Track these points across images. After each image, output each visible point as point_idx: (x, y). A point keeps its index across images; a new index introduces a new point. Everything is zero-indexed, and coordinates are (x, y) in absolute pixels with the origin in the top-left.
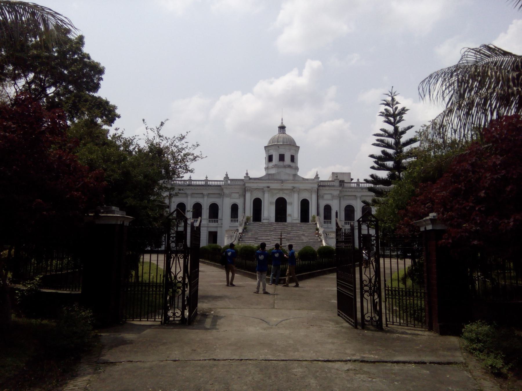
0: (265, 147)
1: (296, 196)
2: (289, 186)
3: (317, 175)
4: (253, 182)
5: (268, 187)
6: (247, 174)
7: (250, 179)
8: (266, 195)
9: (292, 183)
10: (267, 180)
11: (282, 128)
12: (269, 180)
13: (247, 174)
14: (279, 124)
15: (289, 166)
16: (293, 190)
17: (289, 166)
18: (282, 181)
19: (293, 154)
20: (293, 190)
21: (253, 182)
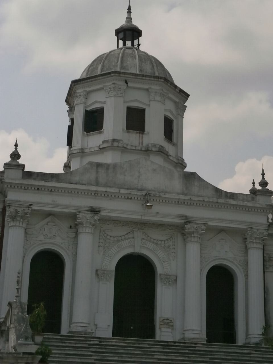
0: (75, 83)
1: (193, 249)
2: (169, 213)
3: (264, 184)
4: (38, 189)
5: (94, 211)
6: (15, 156)
7: (30, 175)
8: (86, 240)
9: (179, 203)
10: (89, 184)
11: (129, 33)
12: (97, 184)
13: (15, 156)
14: (121, 22)
15: (161, 151)
16: (182, 229)
17: (161, 151)
18: (147, 197)
19: (169, 115)
20: (182, 229)
21: (38, 189)
